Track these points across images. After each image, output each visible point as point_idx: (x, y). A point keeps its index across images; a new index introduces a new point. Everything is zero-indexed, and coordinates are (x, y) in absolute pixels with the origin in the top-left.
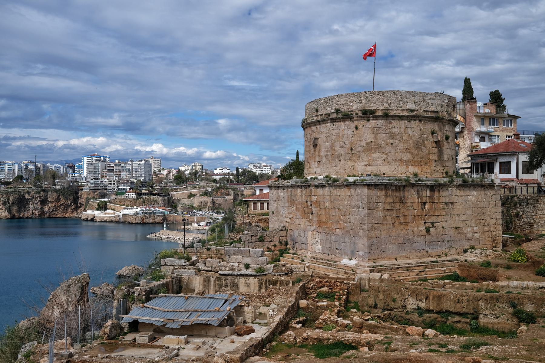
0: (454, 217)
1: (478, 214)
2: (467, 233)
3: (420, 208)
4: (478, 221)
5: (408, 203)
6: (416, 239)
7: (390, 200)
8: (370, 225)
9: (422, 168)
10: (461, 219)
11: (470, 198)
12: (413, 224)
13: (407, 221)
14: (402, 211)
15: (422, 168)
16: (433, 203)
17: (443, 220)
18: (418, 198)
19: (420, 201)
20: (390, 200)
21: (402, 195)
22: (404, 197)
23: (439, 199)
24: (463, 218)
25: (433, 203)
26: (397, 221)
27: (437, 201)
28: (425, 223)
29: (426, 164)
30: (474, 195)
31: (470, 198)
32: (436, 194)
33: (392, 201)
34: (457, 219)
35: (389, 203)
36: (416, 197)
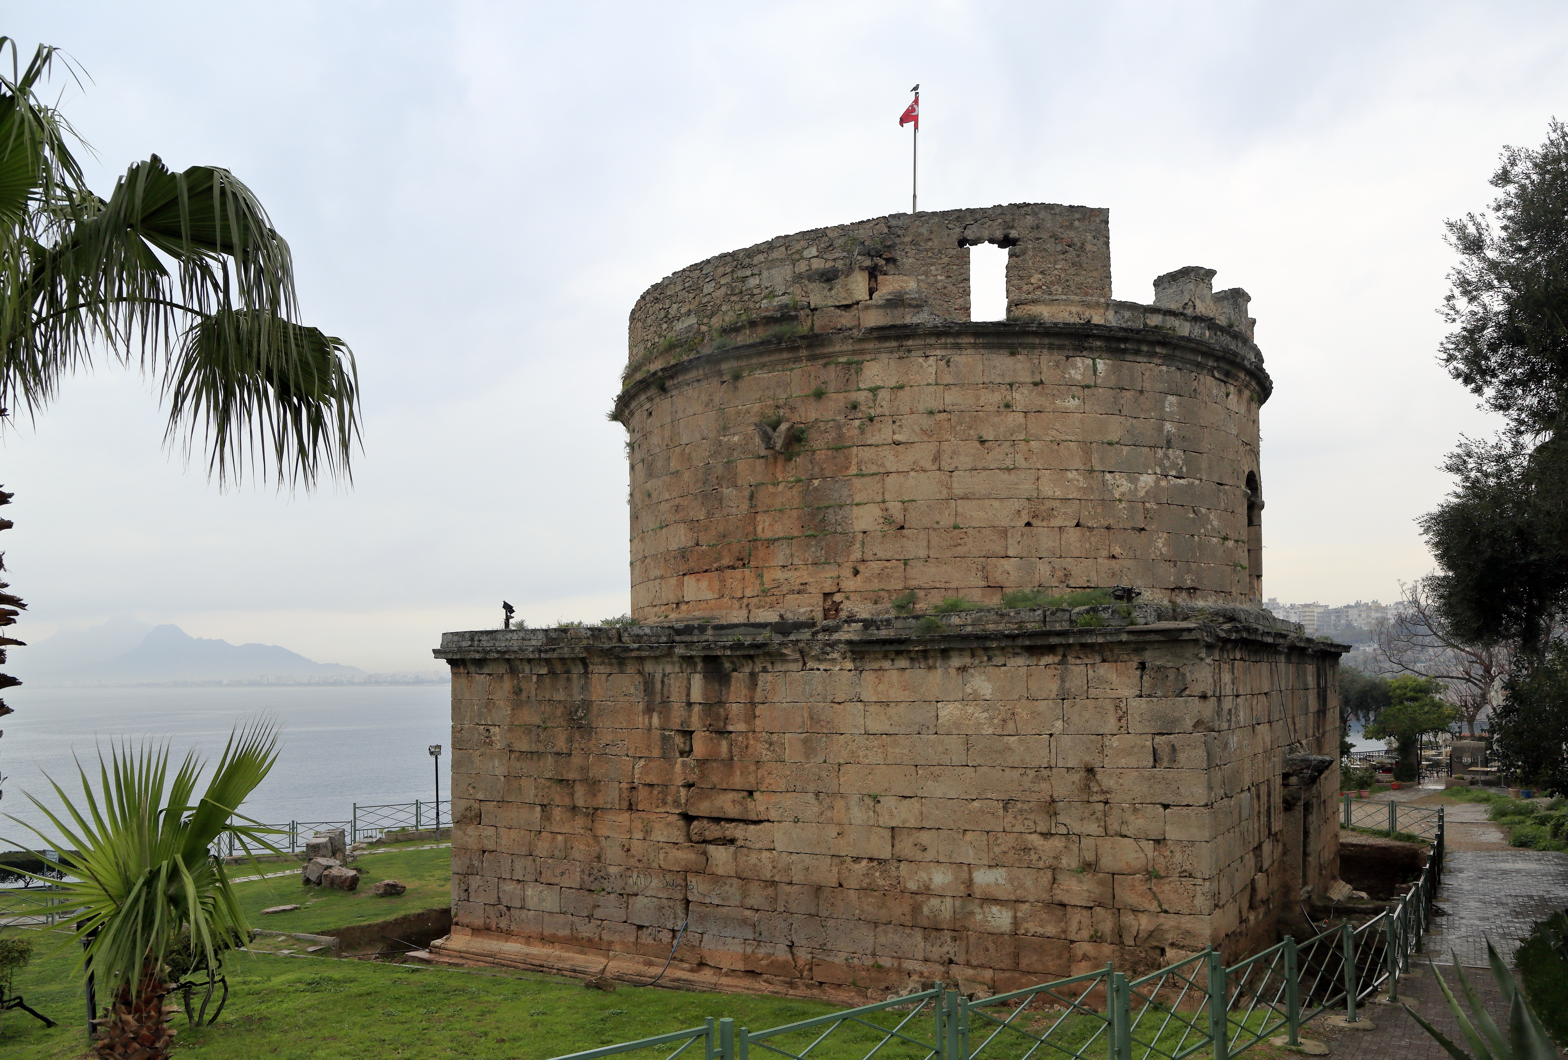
0: (840, 804)
1: (1007, 804)
2: (926, 891)
3: (656, 752)
4: (1009, 841)
5: (606, 730)
6: (636, 881)
7: (530, 716)
8: (463, 804)
9: (723, 581)
10: (886, 820)
11: (948, 712)
12: (624, 818)
13: (600, 801)
14: (577, 760)
15: (723, 581)
16: (722, 733)
17: (773, 815)
18: (649, 710)
19: (656, 721)
20: (530, 716)
21: (578, 698)
22: (586, 705)
23: (751, 717)
24: (905, 814)
25: (722, 733)
26: (557, 801)
27: (741, 727)
28: (688, 818)
29: (742, 561)
30: (976, 698)
31: (948, 712)
32: (737, 691)
33: (536, 720)
34: (858, 815)
35: (528, 729)
36: (641, 706)
